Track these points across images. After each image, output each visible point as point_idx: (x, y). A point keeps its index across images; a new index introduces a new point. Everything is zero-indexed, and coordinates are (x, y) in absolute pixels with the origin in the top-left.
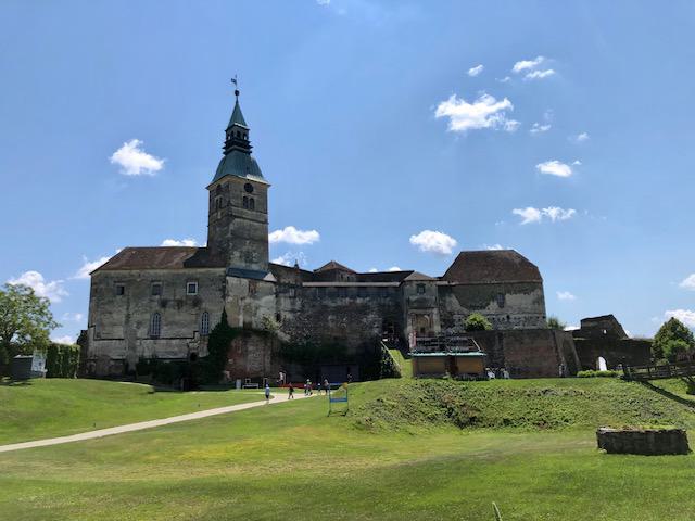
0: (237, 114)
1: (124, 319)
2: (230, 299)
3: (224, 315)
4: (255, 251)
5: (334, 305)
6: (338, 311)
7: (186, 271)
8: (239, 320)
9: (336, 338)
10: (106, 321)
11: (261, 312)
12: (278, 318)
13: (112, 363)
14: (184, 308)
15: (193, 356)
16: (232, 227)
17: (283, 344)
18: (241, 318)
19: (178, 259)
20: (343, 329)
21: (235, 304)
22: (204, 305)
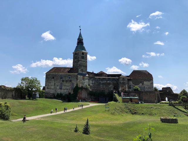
0: (80, 35)
1: (54, 84)
2: (78, 81)
3: (77, 84)
5: (102, 82)
6: (103, 84)
7: (68, 74)
8: (80, 85)
9: (102, 90)
10: (49, 85)
11: (85, 84)
12: (89, 85)
13: (51, 94)
14: (68, 82)
15: (70, 93)
16: (79, 63)
17: (90, 91)
18: (81, 85)
19: (67, 70)
20: (104, 88)
21: (79, 82)
22: (72, 82)
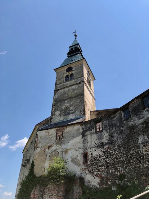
2: (38, 150)
4: (72, 105)
